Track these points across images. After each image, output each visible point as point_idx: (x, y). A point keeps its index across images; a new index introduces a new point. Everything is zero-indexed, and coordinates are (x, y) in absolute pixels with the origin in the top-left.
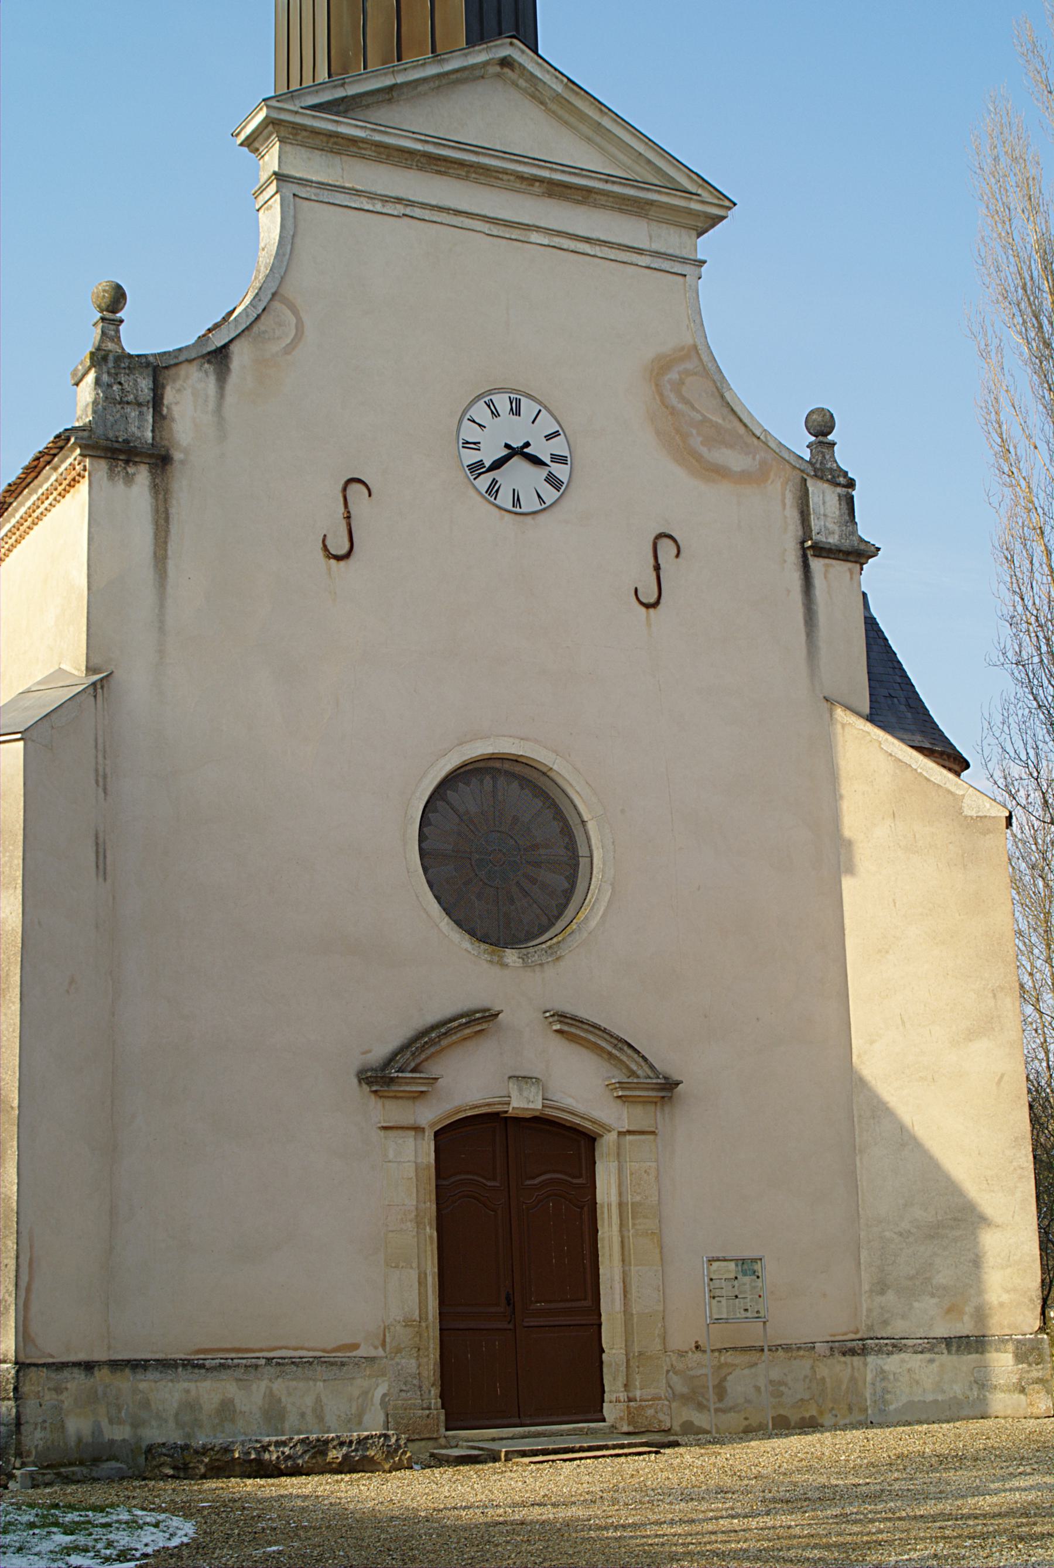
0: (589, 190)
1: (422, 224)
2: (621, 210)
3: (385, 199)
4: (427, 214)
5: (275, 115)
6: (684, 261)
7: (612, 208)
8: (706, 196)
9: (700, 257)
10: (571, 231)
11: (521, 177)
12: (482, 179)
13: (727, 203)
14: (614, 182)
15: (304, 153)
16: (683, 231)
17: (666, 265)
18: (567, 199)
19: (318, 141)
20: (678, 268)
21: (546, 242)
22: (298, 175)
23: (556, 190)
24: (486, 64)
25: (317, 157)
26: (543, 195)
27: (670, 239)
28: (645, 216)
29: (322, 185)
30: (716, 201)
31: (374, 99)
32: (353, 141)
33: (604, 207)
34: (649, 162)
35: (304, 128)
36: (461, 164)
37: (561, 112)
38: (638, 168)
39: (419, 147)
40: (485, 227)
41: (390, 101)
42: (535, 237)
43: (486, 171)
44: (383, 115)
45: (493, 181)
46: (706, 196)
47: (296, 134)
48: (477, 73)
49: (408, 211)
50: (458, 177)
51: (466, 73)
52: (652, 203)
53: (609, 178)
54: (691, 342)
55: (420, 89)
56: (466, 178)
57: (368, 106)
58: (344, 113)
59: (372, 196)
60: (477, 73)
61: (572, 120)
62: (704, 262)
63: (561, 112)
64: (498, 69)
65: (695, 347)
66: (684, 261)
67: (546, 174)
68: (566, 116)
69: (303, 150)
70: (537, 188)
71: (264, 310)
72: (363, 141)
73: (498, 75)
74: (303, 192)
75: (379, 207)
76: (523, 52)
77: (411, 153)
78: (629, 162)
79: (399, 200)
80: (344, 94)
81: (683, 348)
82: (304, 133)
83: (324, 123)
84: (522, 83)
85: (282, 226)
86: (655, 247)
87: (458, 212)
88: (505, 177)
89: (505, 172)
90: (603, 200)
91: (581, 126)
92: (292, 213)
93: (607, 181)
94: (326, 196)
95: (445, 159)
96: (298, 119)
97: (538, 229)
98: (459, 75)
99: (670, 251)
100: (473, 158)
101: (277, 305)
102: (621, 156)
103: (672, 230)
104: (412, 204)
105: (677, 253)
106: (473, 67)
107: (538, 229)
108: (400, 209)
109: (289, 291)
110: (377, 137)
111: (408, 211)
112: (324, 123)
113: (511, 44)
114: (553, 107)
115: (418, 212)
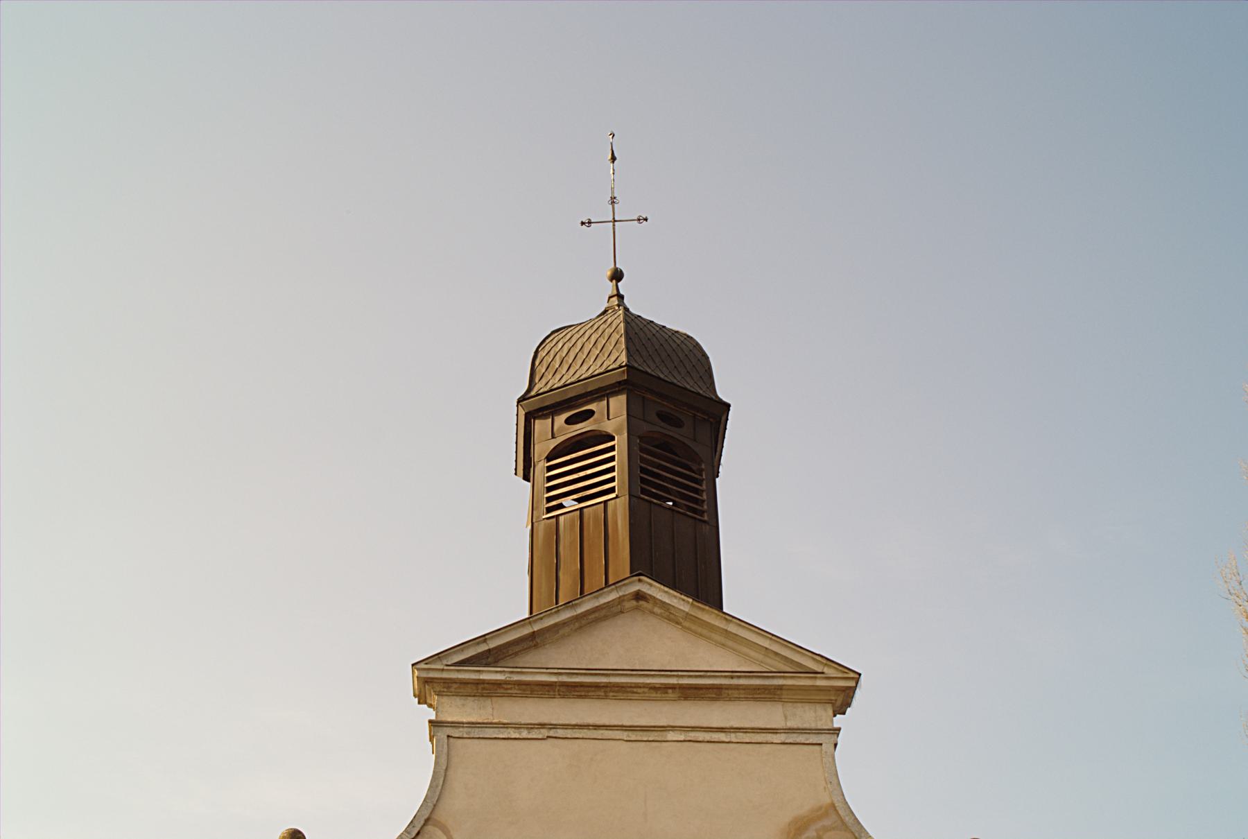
0: (719, 688)
1: (566, 742)
2: (755, 699)
3: (531, 727)
4: (569, 733)
5: (424, 675)
6: (819, 731)
7: (747, 699)
8: (829, 671)
9: (836, 726)
10: (705, 725)
11: (653, 688)
12: (620, 695)
13: (852, 675)
14: (739, 677)
15: (458, 701)
16: (818, 707)
17: (801, 738)
18: (702, 699)
19: (469, 689)
20: (813, 739)
21: (682, 738)
22: (449, 719)
23: (689, 693)
24: (621, 600)
25: (470, 702)
26: (679, 698)
27: (808, 716)
28: (780, 700)
29: (472, 725)
30: (840, 675)
31: (517, 649)
32: (498, 684)
33: (738, 699)
34: (776, 654)
35: (454, 681)
36: (597, 686)
37: (694, 627)
38: (768, 661)
39: (553, 679)
40: (624, 735)
41: (536, 646)
42: (671, 736)
43: (621, 688)
44: (531, 659)
45: (630, 696)
46: (829, 671)
47: (449, 687)
48: (615, 610)
49: (552, 733)
50: (599, 698)
51: (603, 612)
52: (781, 688)
53: (733, 674)
54: (828, 801)
55: (561, 632)
56: (606, 697)
57: (516, 654)
58: (495, 663)
59: (518, 726)
60: (615, 610)
61: (705, 632)
62: (839, 729)
63: (694, 627)
64: (634, 603)
65: (833, 806)
66: (819, 731)
67: (673, 681)
68: (700, 630)
69: (458, 699)
70: (671, 694)
71: (418, 833)
72: (506, 682)
73: (637, 608)
74: (455, 732)
75: (525, 734)
76: (651, 585)
77: (550, 685)
78: (761, 657)
79: (542, 726)
80: (486, 648)
81: (820, 808)
82: (455, 686)
83: (468, 674)
84: (657, 610)
85: (436, 763)
86: (790, 724)
87: (597, 727)
88: (639, 690)
89: (637, 686)
90: (735, 694)
91: (713, 635)
92: (445, 750)
93: (732, 677)
94: (476, 732)
95: (582, 685)
96: (445, 675)
97: (673, 728)
98: (597, 615)
99: (806, 726)
100: (604, 680)
101: (429, 828)
102: (752, 653)
103: (807, 706)
104: (554, 726)
105: (813, 726)
106: (608, 605)
107: (673, 728)
108: (545, 733)
109: (441, 815)
110: (516, 678)
111: (552, 733)
112: (468, 674)
113: (640, 580)
114: (687, 624)
115: (560, 733)
